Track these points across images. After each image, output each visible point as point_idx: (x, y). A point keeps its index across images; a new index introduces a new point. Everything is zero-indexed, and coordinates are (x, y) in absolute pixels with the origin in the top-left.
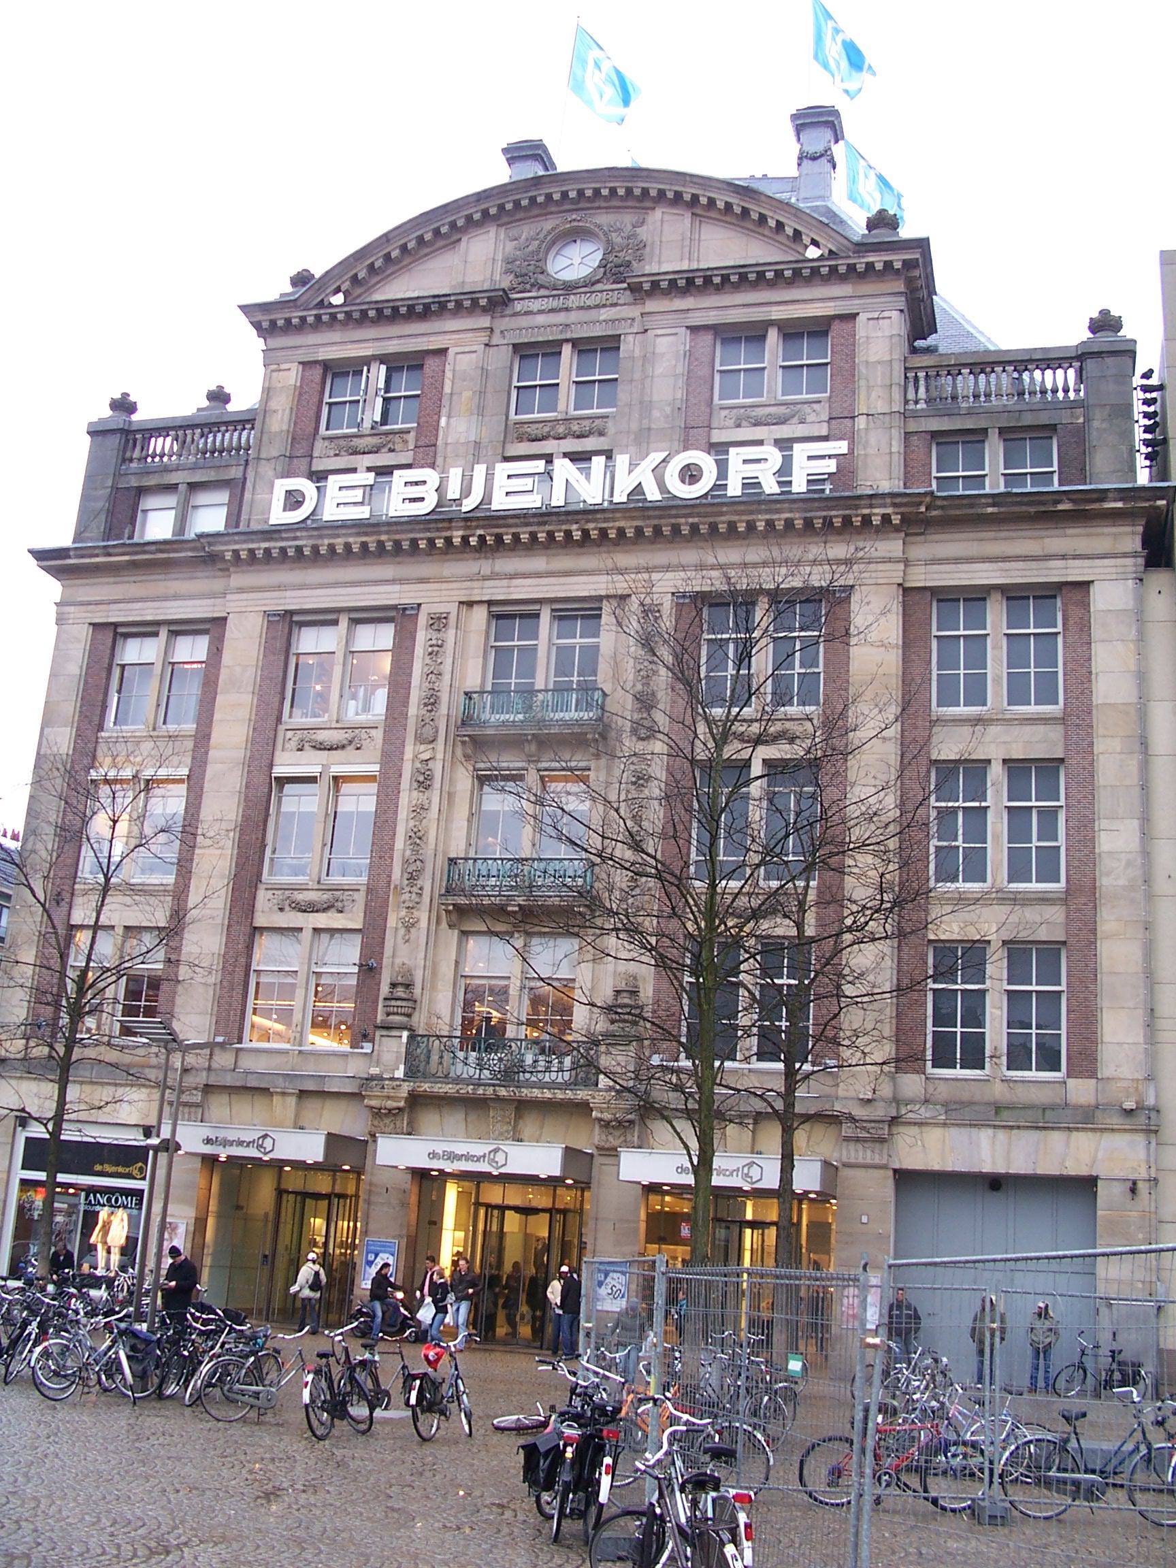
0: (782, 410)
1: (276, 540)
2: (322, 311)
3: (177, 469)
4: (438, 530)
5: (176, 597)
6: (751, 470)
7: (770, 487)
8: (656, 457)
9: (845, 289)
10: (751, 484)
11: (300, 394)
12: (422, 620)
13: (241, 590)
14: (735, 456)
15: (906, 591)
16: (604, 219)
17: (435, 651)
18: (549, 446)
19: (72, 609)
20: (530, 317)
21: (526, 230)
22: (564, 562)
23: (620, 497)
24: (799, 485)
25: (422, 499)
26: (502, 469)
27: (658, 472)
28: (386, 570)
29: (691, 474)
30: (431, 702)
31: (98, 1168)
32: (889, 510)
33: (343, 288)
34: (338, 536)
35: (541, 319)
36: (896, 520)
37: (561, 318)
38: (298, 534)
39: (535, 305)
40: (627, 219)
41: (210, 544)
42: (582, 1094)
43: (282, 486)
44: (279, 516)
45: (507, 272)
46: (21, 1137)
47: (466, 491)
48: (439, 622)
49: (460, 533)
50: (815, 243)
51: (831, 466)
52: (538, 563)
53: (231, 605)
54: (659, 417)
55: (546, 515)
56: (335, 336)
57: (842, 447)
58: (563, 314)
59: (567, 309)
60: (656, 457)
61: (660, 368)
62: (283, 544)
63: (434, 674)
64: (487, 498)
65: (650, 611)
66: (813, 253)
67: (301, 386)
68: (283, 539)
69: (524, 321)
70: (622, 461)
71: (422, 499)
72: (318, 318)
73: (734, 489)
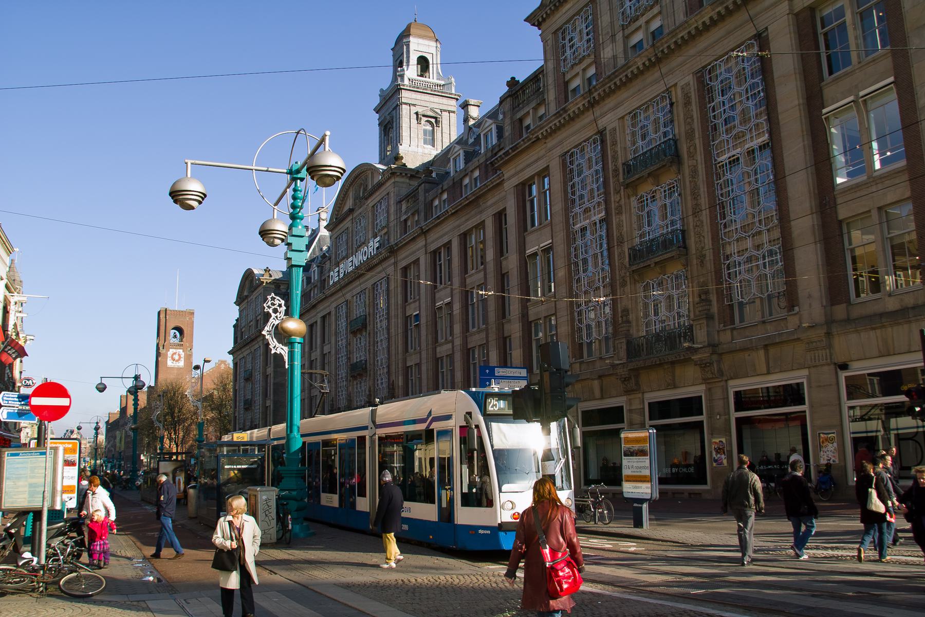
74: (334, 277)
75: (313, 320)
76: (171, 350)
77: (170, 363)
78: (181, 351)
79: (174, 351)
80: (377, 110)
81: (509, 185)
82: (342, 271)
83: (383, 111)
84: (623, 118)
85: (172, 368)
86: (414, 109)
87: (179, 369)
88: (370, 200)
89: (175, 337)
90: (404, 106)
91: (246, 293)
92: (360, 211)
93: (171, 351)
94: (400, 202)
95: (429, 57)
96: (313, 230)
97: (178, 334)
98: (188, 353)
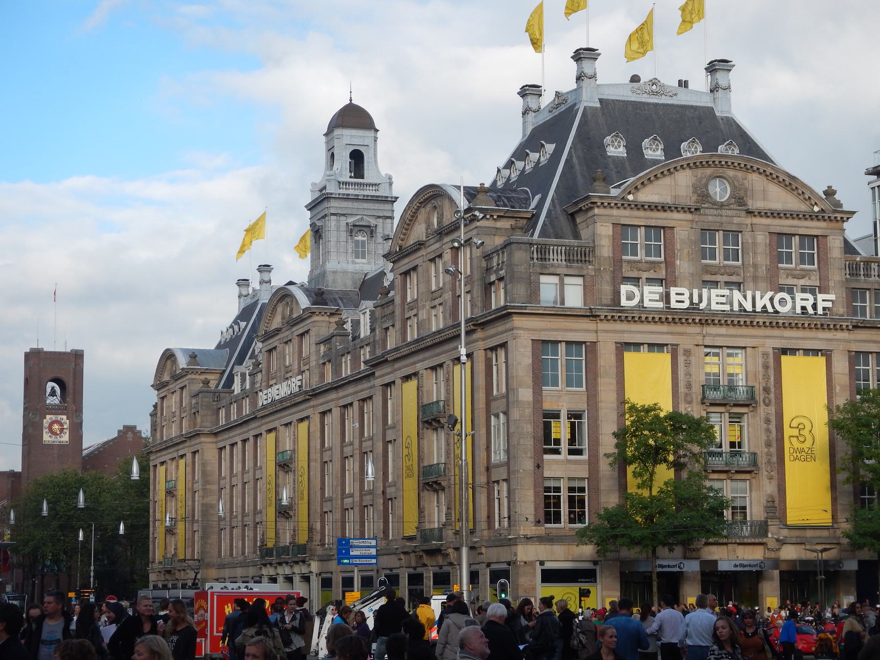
0: (803, 273)
1: (625, 313)
2: (625, 202)
3: (559, 266)
4: (691, 316)
5: (571, 330)
6: (804, 303)
7: (811, 311)
8: (770, 294)
9: (822, 224)
10: (804, 308)
11: (613, 239)
12: (680, 352)
13: (606, 331)
14: (799, 296)
15: (849, 351)
16: (731, 173)
17: (688, 364)
18: (718, 278)
19: (522, 332)
20: (706, 217)
21: (700, 172)
22: (732, 331)
23: (758, 309)
24: (820, 311)
25: (683, 302)
26: (714, 292)
27: (771, 300)
28: (664, 328)
29: (782, 302)
30: (689, 386)
31: (580, 580)
32: (849, 324)
33: (632, 192)
34: (650, 314)
35: (710, 218)
36: (850, 327)
37: (718, 219)
38: (635, 312)
39: (707, 211)
40: (740, 174)
41: (595, 312)
42: (765, 540)
43: (624, 289)
44: (624, 302)
45: (694, 192)
46: (539, 569)
47: (701, 301)
48: (687, 353)
49: (699, 318)
50: (816, 204)
51: (829, 305)
52: (723, 330)
53: (602, 337)
54: (762, 271)
55: (730, 314)
56: (627, 212)
57: (832, 297)
58: (719, 217)
59: (721, 216)
60: (770, 294)
61: (761, 249)
62: (626, 315)
63: (688, 374)
64: (709, 304)
65: (765, 355)
66: (816, 209)
67: (613, 235)
68: (628, 313)
69: (702, 218)
70: (758, 294)
71: (683, 302)
72: (623, 205)
73: (799, 310)
74: (263, 399)
75: (245, 436)
76: (48, 417)
77: (47, 437)
78: (65, 417)
79: (54, 417)
80: (311, 207)
81: (378, 382)
82: (269, 395)
83: (316, 211)
84: (426, 369)
85: (50, 446)
86: (343, 221)
87: (61, 446)
88: (294, 329)
89: (53, 393)
90: (333, 217)
91: (166, 378)
92: (287, 333)
93: (49, 418)
94: (318, 344)
95: (362, 149)
96: (254, 290)
97: (58, 389)
98: (76, 420)
